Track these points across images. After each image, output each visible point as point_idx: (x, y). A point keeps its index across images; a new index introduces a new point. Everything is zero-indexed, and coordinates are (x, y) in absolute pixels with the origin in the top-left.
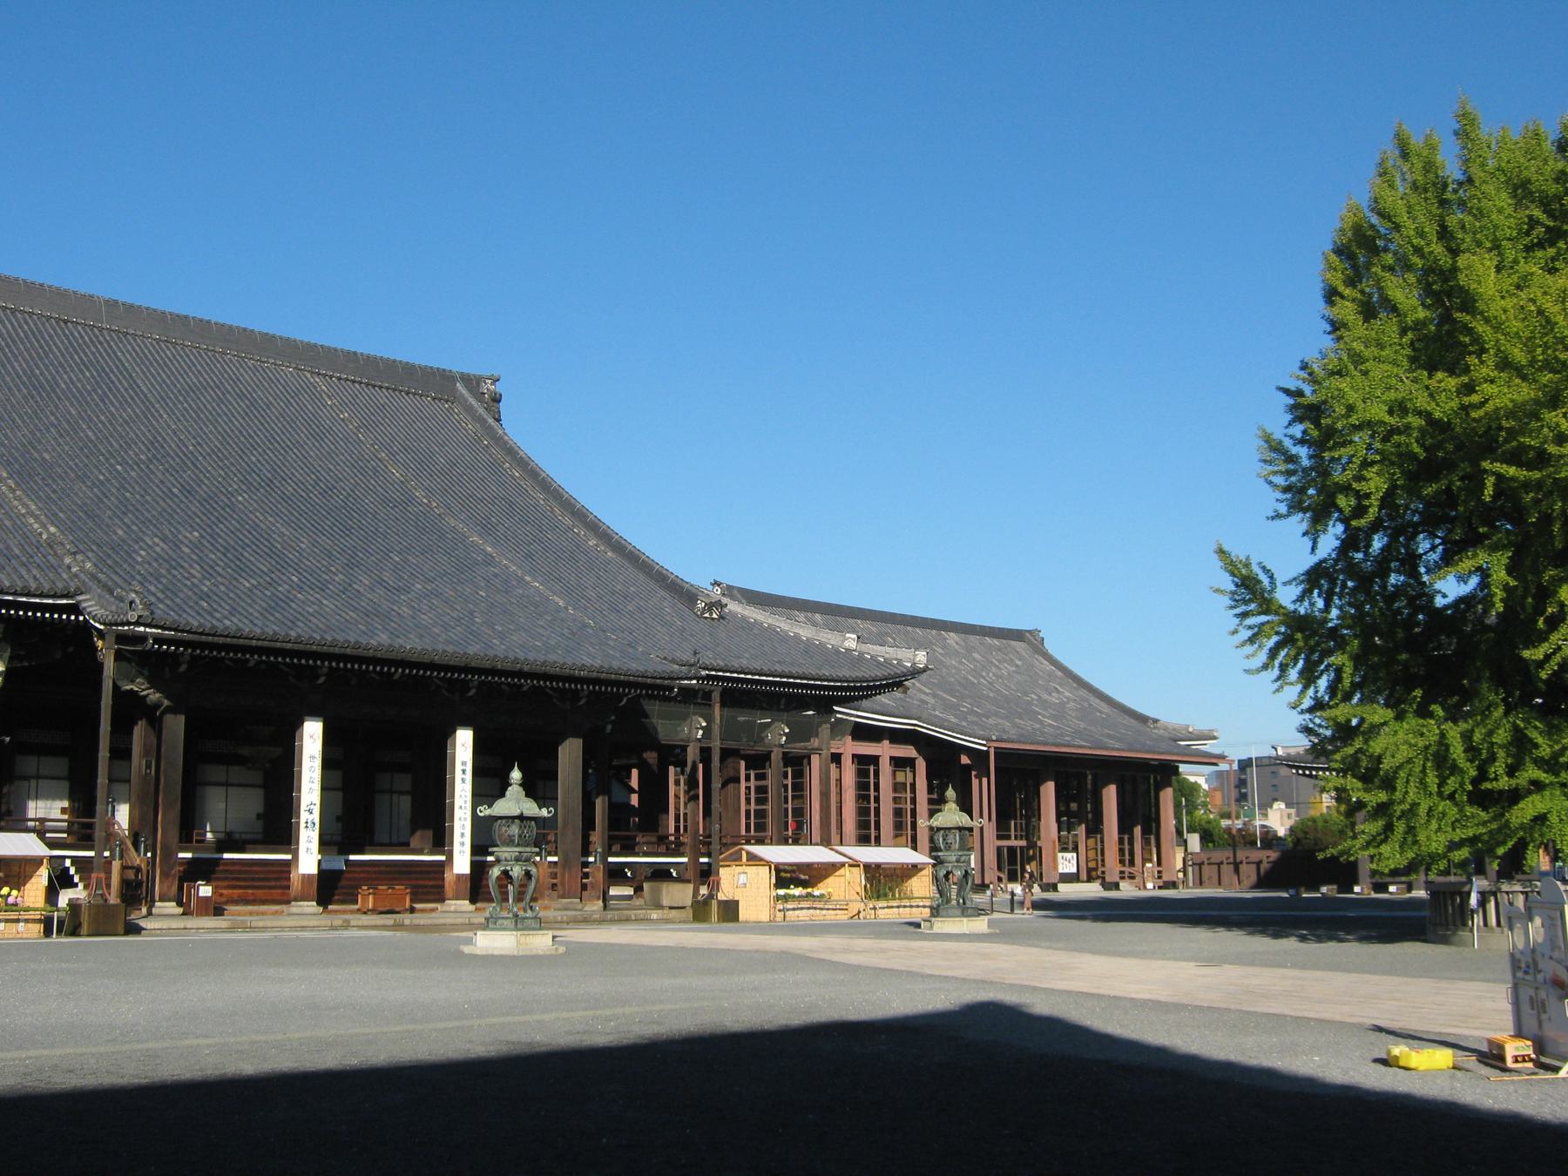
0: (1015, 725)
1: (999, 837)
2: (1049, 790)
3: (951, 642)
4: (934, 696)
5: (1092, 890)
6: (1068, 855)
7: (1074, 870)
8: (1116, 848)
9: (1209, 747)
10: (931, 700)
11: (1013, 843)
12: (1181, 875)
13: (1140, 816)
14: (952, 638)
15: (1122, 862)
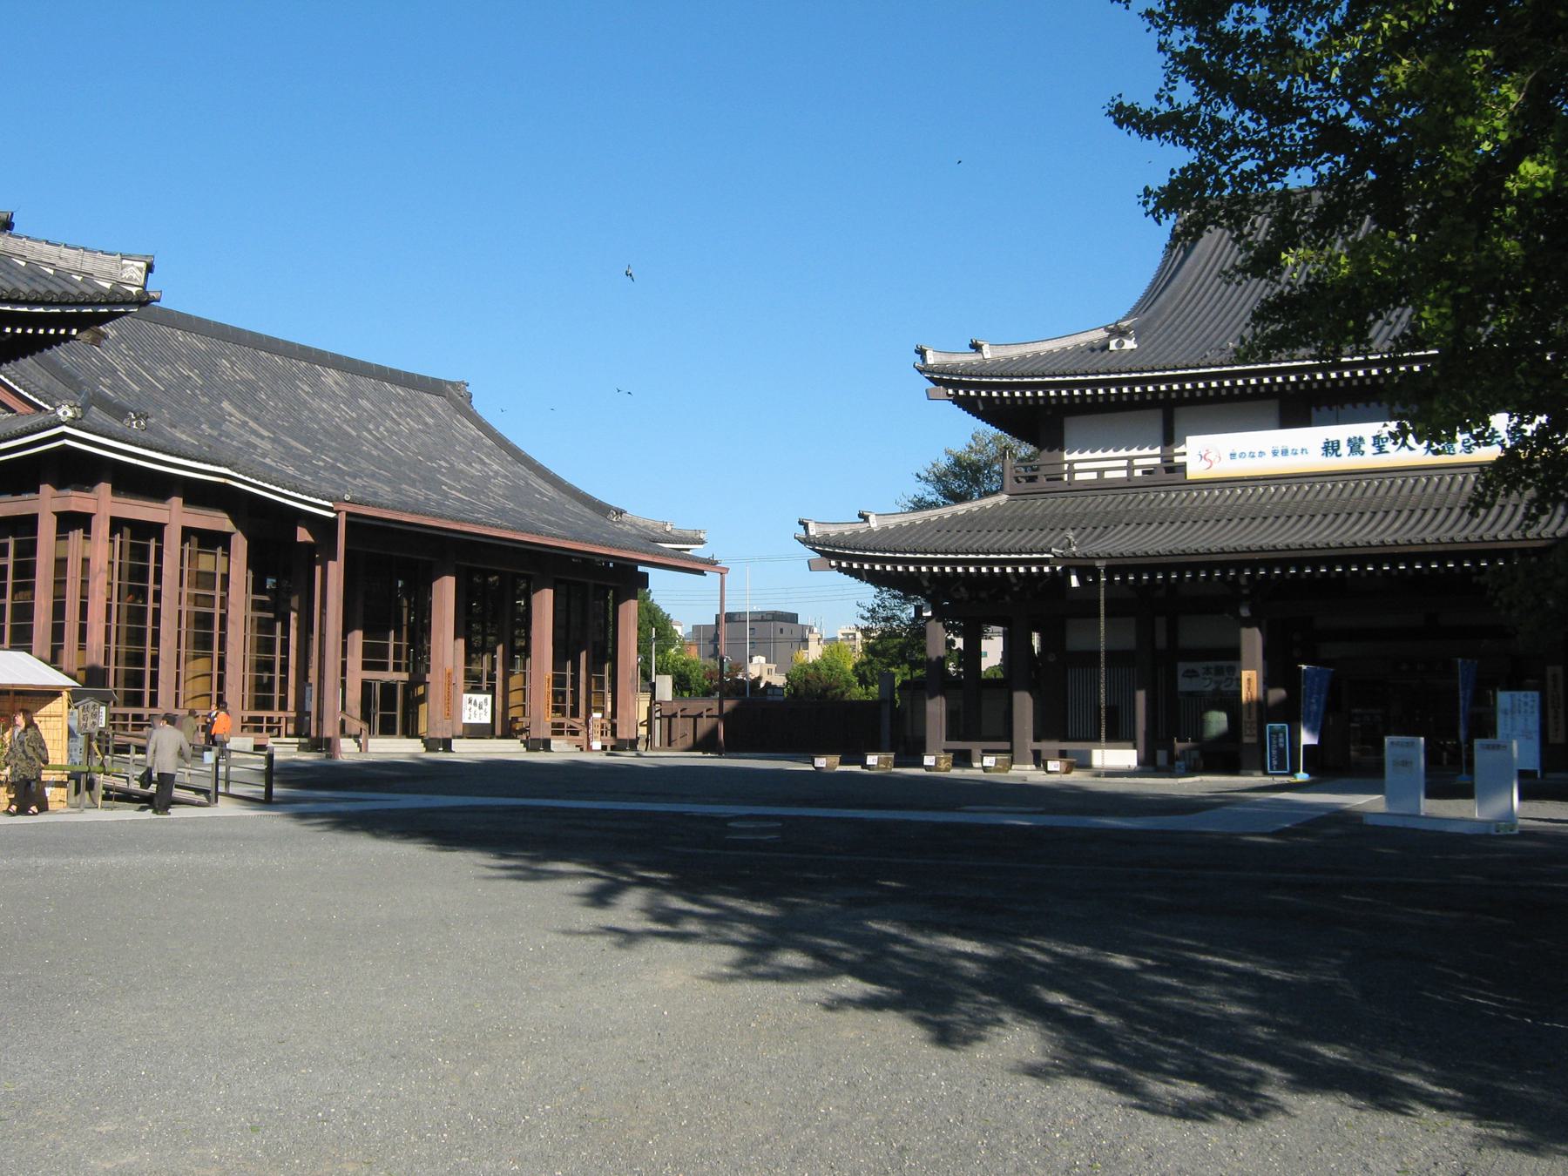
0: (400, 491)
1: (366, 666)
2: (445, 591)
3: (330, 381)
4: (274, 441)
5: (510, 750)
6: (480, 698)
7: (488, 720)
8: (548, 689)
9: (697, 550)
10: (267, 445)
11: (390, 676)
12: (643, 731)
13: (587, 642)
14: (331, 377)
15: (556, 709)
